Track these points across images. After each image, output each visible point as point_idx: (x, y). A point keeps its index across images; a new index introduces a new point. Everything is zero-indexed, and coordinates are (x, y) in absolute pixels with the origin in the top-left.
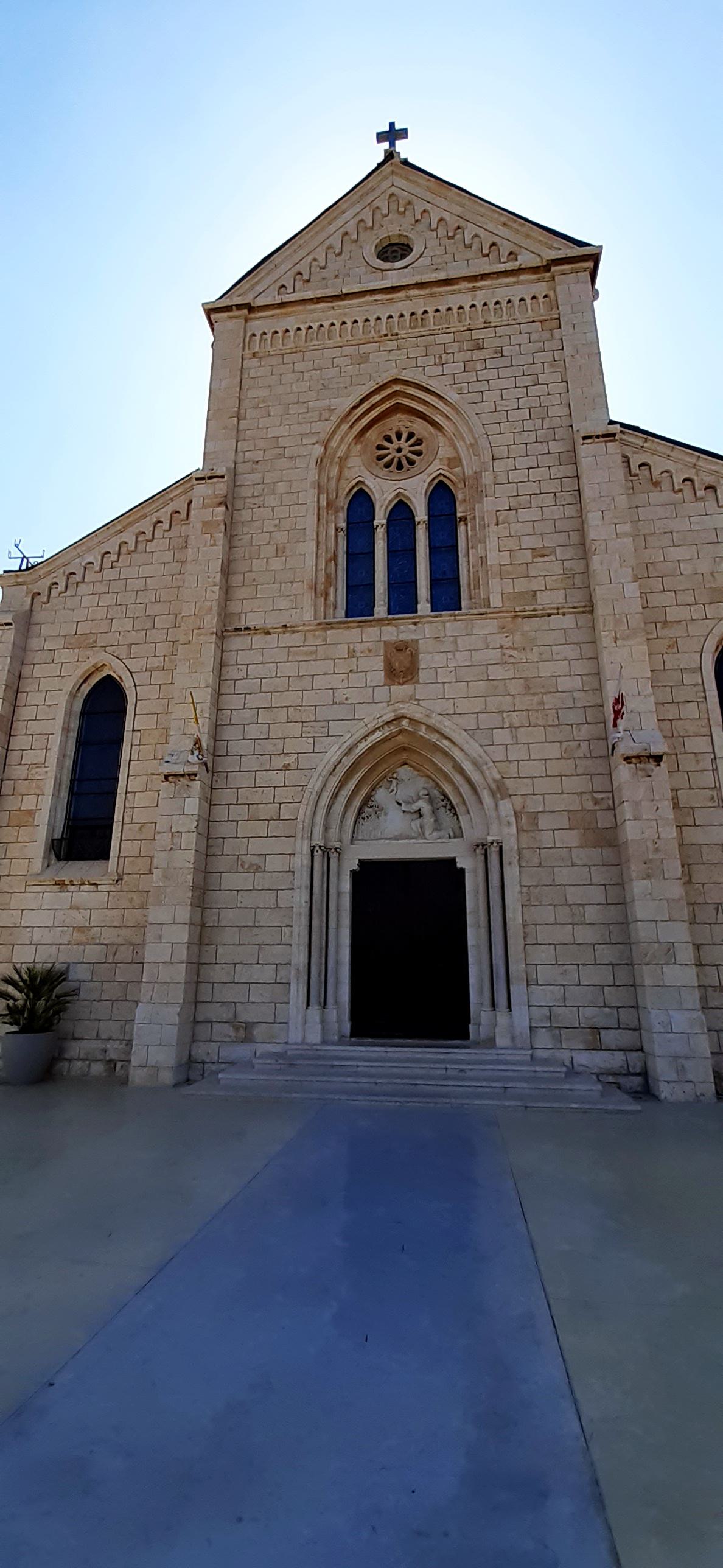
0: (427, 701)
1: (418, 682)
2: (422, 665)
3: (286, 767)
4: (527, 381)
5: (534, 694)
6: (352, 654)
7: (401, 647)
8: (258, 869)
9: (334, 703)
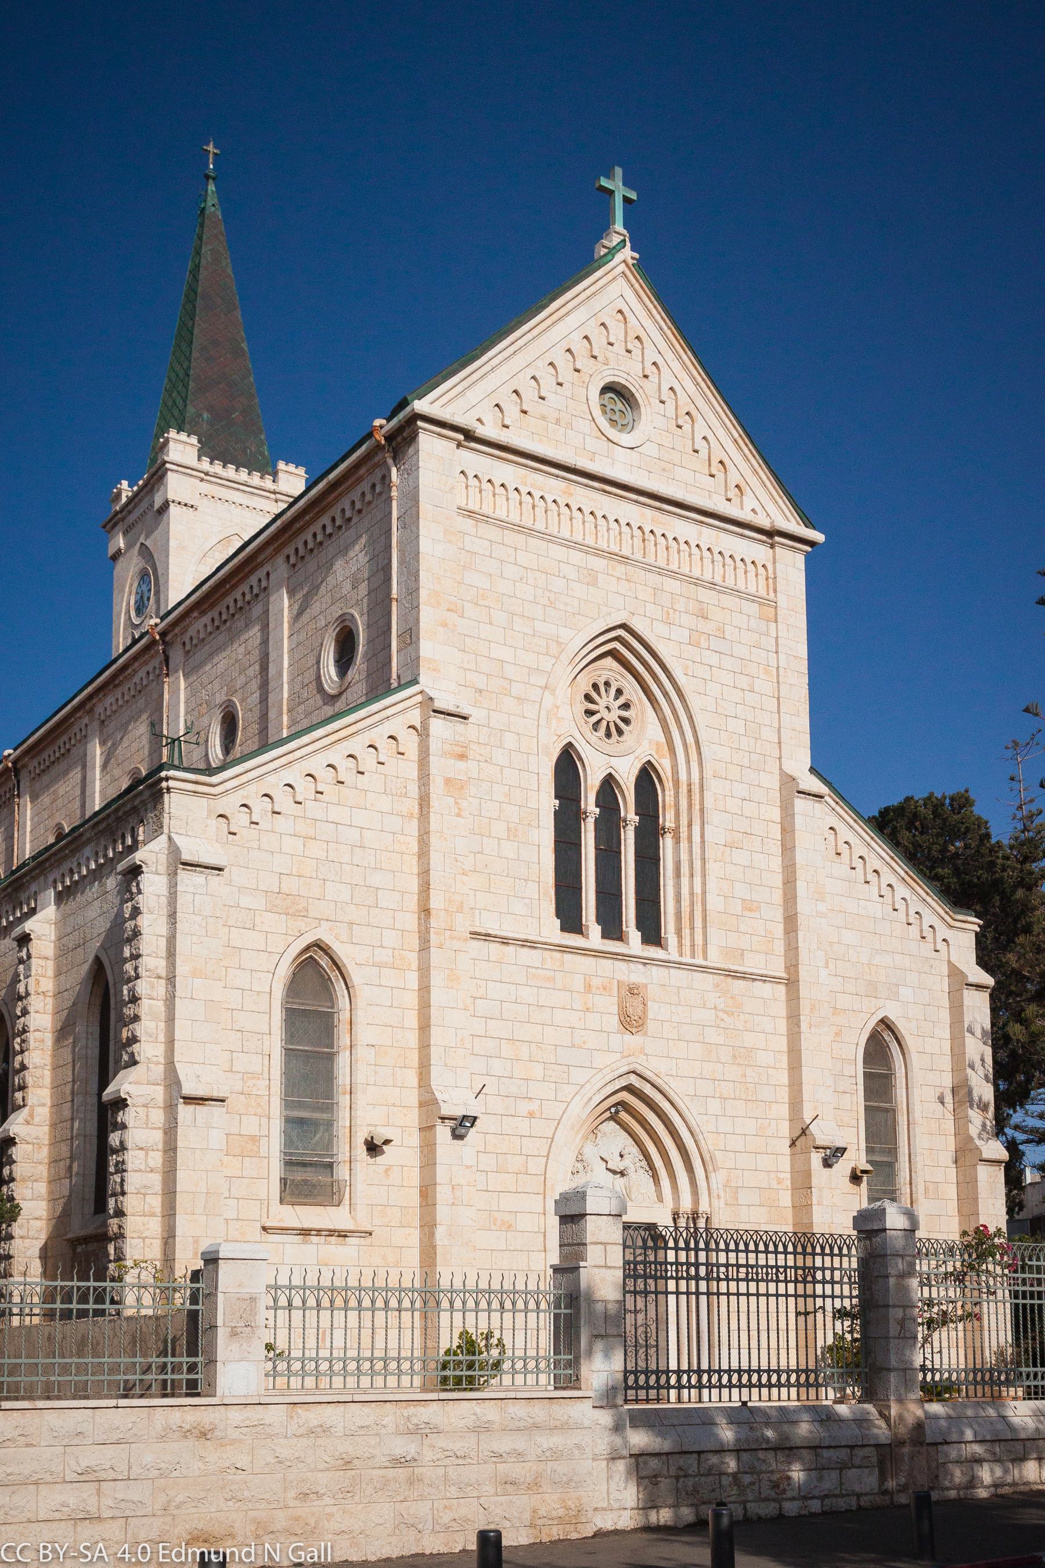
0: (669, 1061)
1: (646, 1034)
2: (650, 1015)
3: (531, 1115)
4: (743, 682)
5: (739, 1065)
6: (588, 988)
7: (633, 991)
8: (510, 1227)
9: (573, 1046)
